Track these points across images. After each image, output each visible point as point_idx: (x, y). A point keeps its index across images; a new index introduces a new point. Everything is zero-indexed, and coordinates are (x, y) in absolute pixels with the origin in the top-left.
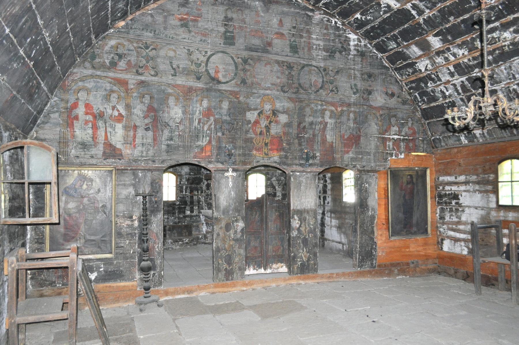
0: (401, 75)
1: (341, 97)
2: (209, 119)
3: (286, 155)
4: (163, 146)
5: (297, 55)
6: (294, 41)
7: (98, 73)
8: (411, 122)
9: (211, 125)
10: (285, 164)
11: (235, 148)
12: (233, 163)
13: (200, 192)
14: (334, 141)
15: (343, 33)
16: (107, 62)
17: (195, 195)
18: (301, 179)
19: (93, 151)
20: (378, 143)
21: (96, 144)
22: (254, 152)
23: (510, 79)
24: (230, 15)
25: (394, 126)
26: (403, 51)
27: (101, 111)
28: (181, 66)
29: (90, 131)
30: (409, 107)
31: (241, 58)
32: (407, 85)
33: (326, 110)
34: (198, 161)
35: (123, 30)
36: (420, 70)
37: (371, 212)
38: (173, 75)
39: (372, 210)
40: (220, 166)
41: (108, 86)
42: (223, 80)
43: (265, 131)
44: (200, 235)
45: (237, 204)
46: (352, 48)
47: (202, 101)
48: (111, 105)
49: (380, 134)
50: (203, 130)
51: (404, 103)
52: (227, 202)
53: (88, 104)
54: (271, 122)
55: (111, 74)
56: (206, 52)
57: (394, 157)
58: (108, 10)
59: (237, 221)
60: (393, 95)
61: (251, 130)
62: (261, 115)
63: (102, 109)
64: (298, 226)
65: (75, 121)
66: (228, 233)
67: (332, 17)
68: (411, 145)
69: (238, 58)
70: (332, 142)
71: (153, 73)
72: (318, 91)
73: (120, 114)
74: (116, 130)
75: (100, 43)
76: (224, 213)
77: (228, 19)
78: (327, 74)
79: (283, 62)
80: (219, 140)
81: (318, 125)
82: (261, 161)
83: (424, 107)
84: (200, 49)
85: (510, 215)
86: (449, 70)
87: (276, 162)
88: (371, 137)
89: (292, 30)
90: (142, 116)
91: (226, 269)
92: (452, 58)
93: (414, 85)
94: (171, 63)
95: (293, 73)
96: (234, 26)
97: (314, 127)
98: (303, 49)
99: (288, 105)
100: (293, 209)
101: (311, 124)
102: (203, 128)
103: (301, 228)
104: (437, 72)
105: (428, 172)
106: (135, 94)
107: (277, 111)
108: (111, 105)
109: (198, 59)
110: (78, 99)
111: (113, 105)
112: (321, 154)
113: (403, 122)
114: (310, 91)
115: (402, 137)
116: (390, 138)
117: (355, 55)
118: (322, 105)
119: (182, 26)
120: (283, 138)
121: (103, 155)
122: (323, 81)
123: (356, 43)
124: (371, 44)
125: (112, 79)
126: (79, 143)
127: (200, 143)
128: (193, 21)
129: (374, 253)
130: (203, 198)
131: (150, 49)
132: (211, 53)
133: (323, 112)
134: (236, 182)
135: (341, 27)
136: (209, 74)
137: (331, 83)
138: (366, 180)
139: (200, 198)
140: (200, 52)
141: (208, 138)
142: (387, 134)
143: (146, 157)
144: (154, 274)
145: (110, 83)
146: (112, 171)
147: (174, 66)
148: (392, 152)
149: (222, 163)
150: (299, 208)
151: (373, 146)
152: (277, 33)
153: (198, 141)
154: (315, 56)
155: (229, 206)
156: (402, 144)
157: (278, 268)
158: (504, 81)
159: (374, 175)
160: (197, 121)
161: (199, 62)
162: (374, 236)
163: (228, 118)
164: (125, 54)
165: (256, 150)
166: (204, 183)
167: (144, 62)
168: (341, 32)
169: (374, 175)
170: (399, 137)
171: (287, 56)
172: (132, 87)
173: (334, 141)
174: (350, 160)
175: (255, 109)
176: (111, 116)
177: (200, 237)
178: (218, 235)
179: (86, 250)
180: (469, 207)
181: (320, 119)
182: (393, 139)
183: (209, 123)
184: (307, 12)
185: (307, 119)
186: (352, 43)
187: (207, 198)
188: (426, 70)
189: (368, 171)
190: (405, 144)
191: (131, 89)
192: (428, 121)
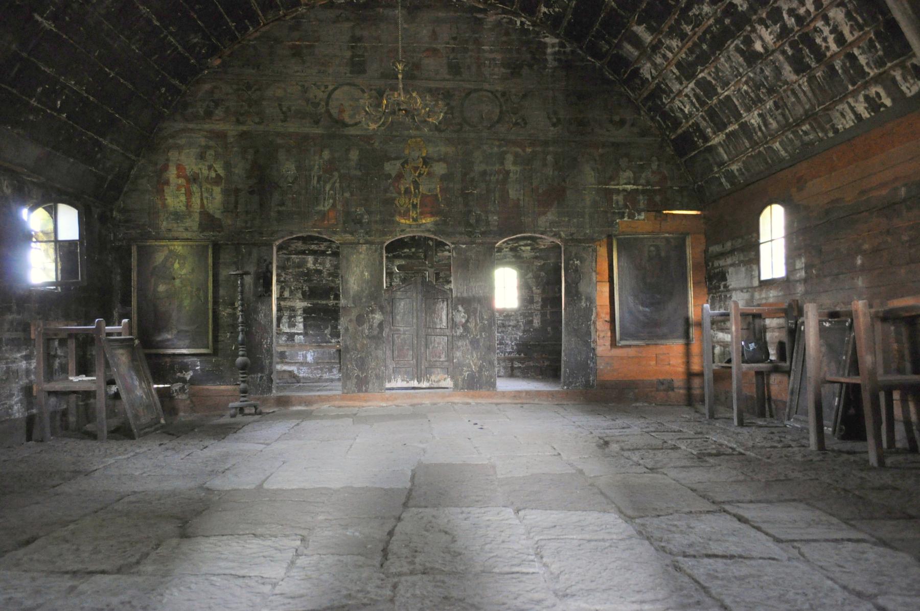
0: (633, 90)
1: (532, 131)
2: (331, 175)
3: (445, 221)
4: (272, 214)
5: (458, 78)
6: (454, 58)
7: (191, 126)
8: (657, 163)
9: (335, 183)
10: (443, 233)
11: (369, 213)
12: (367, 233)
14: (522, 198)
15: (534, 38)
16: (201, 112)
18: (469, 254)
19: (188, 223)
20: (598, 198)
21: (190, 214)
22: (397, 218)
23: (736, 76)
24: (358, 33)
25: (625, 171)
26: (618, 53)
27: (195, 172)
28: (293, 108)
29: (183, 198)
30: (654, 139)
31: (375, 90)
32: (644, 105)
33: (505, 153)
34: (319, 232)
35: (220, 70)
36: (647, 79)
37: (586, 302)
38: (283, 121)
39: (587, 299)
40: (349, 237)
41: (203, 142)
42: (351, 122)
43: (412, 187)
45: (373, 289)
46: (550, 58)
47: (322, 151)
48: (207, 163)
49: (599, 183)
50: (325, 190)
51: (644, 133)
52: (358, 286)
53: (179, 165)
54: (420, 175)
55: (207, 126)
56: (326, 87)
57: (626, 219)
58: (177, 48)
59: (372, 312)
60: (622, 123)
61: (391, 188)
62: (406, 166)
63: (196, 170)
64: (464, 320)
65: (165, 187)
66: (360, 328)
67: (516, 17)
68: (658, 198)
69: (371, 90)
70: (518, 199)
71: (257, 120)
72: (492, 126)
73: (218, 175)
74: (214, 195)
75: (192, 88)
76: (354, 302)
77: (356, 39)
78: (507, 100)
79: (437, 89)
80: (346, 203)
81: (495, 175)
82: (408, 230)
83: (673, 137)
84: (319, 84)
85: (771, 295)
86: (674, 74)
87: (429, 231)
88: (584, 189)
89: (452, 42)
90: (245, 176)
91: (358, 376)
92: (670, 55)
93: (650, 104)
94: (280, 105)
95: (453, 103)
96: (365, 48)
97: (488, 178)
98: (469, 67)
99: (444, 149)
100: (456, 297)
101: (484, 173)
102: (324, 188)
103: (469, 324)
104: (664, 79)
105: (688, 241)
106: (235, 149)
107: (428, 158)
108: (207, 163)
109: (315, 96)
110: (168, 160)
111: (209, 164)
112: (499, 218)
113: (642, 163)
114: (480, 127)
115: (640, 187)
116: (618, 189)
117: (555, 68)
118: (499, 146)
119: (294, 55)
120: (439, 196)
121: (199, 228)
122: (501, 112)
123: (557, 49)
124: (581, 48)
125: (207, 132)
126: (171, 213)
127: (321, 208)
128: (307, 47)
129: (592, 365)
131: (253, 89)
132: (333, 87)
133: (501, 159)
134: (371, 258)
135: (531, 28)
136: (330, 115)
137: (515, 114)
138: (576, 254)
140: (318, 87)
141: (331, 201)
142: (612, 183)
143: (251, 228)
144: (262, 377)
145: (206, 137)
146: (207, 247)
147: (284, 109)
148: (623, 210)
149: (352, 233)
150: (465, 295)
151: (588, 201)
152: (427, 50)
153: (318, 205)
154: (488, 76)
155: (362, 291)
156: (641, 197)
157: (439, 381)
158: (732, 80)
159: (589, 247)
160: (316, 178)
161: (317, 100)
162: (591, 339)
163: (358, 173)
164: (223, 100)
165: (400, 214)
167: (246, 108)
168: (531, 36)
169: (589, 247)
170: (635, 187)
171: (444, 80)
172: (232, 140)
173: (522, 198)
174: (548, 224)
175: (397, 158)
176: (208, 177)
178: (347, 329)
179: (181, 343)
180: (735, 290)
181: (497, 167)
182: (624, 190)
183: (332, 181)
184: (475, 14)
185: (476, 168)
186: (549, 50)
188: (653, 78)
189: (579, 241)
190: (646, 197)
191: (231, 143)
192: (683, 160)
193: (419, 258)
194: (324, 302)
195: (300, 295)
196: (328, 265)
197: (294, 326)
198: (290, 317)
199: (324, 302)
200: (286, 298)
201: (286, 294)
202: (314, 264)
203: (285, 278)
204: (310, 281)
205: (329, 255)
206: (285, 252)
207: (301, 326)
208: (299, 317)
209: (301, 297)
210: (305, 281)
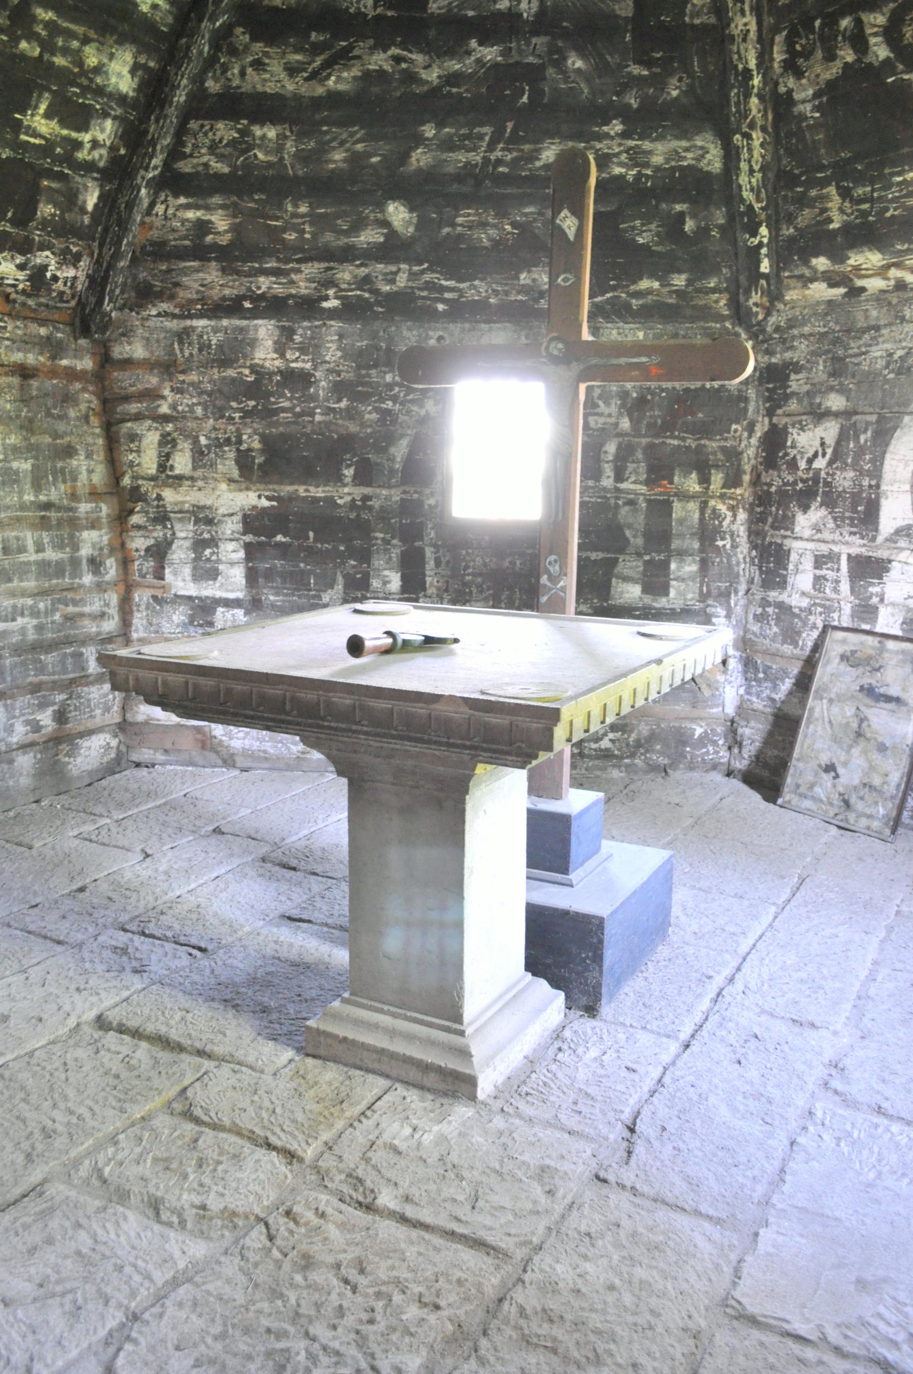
13: (717, 479)
17: (686, 497)
44: (693, 720)
130: (742, 516)
139: (716, 514)
166: (751, 429)
177: (699, 731)
187: (762, 519)
193: (705, 313)
194: (319, 492)
195: (228, 465)
196: (332, 353)
197: (213, 574)
198: (200, 545)
199: (319, 492)
200: (180, 478)
201: (182, 463)
202: (280, 350)
203: (174, 407)
204: (269, 413)
205: (333, 314)
206: (164, 306)
207: (237, 575)
208: (231, 546)
209: (235, 473)
210: (247, 414)
